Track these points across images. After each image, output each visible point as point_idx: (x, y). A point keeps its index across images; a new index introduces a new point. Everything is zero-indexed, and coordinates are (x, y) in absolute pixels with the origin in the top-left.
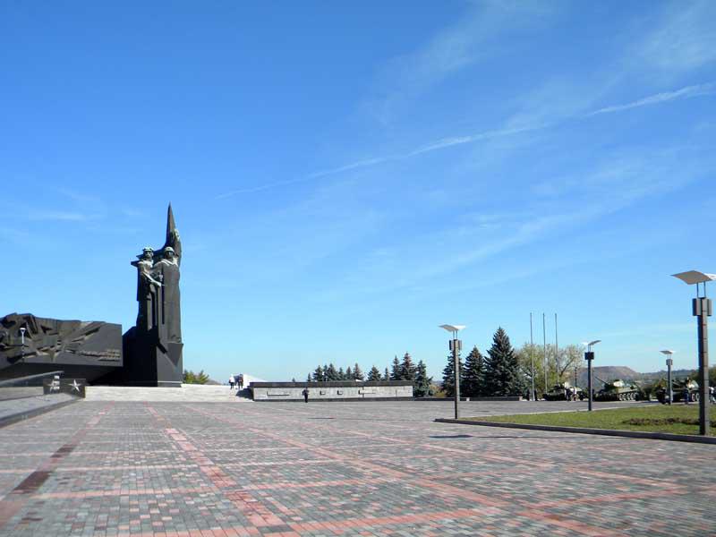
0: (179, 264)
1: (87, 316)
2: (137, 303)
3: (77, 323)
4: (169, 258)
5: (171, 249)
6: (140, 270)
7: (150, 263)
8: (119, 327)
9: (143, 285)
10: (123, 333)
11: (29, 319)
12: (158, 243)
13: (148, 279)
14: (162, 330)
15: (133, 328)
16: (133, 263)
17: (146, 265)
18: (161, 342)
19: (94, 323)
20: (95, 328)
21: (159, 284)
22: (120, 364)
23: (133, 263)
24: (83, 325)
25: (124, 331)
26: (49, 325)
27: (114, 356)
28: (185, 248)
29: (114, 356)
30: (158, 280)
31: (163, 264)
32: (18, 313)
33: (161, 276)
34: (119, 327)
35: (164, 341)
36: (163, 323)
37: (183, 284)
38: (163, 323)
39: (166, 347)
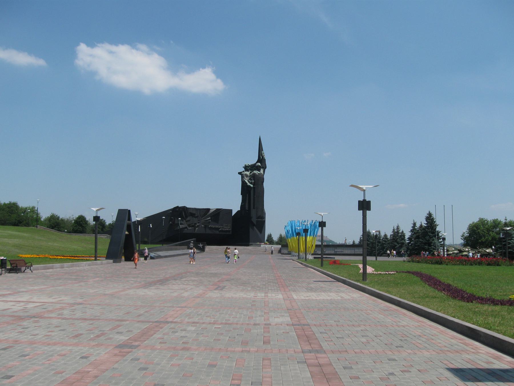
0: (264, 173)
1: (213, 206)
3: (208, 210)
4: (259, 170)
5: (259, 164)
6: (242, 177)
7: (248, 173)
8: (231, 211)
10: (233, 214)
11: (184, 209)
12: (253, 160)
13: (246, 183)
14: (253, 213)
17: (246, 174)
19: (217, 209)
20: (219, 212)
21: (252, 186)
22: (231, 233)
24: (211, 211)
25: (233, 214)
26: (194, 212)
27: (227, 227)
28: (268, 163)
29: (227, 227)
30: (251, 183)
31: (254, 174)
32: (180, 206)
33: (253, 181)
34: (231, 211)
35: (254, 220)
36: (254, 208)
37: (266, 185)
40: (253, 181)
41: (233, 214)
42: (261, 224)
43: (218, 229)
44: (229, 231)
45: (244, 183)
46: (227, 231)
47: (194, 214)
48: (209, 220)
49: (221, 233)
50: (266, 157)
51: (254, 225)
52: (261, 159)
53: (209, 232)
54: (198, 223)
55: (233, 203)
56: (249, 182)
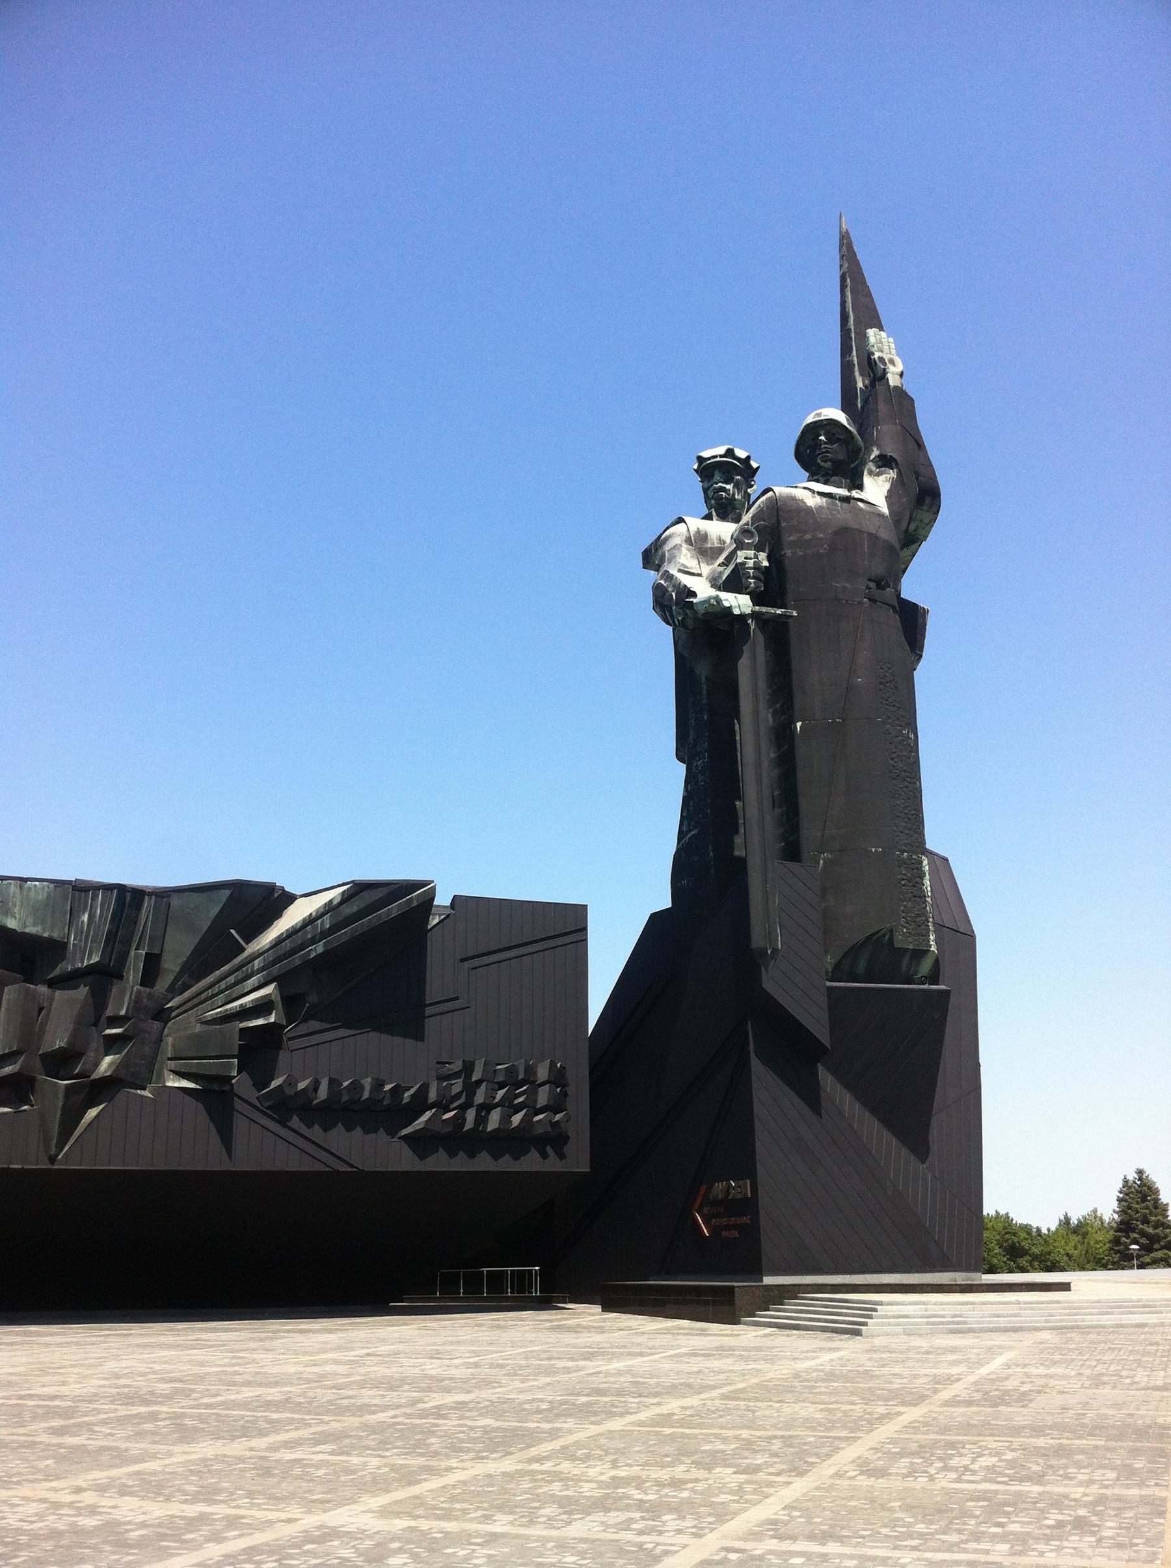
2: (682, 768)
8: (566, 927)
15: (656, 920)
18: (774, 982)
19: (359, 888)
21: (740, 603)
22: (578, 1159)
30: (734, 583)
33: (753, 558)
35: (800, 985)
38: (792, 852)
39: (815, 1020)
40: (753, 558)
43: (387, 1113)
44: (556, 1140)
46: (510, 1142)
47: (57, 948)
48: (262, 1008)
49: (439, 1162)
51: (796, 1054)
53: (264, 1147)
54: (111, 1044)
56: (714, 583)
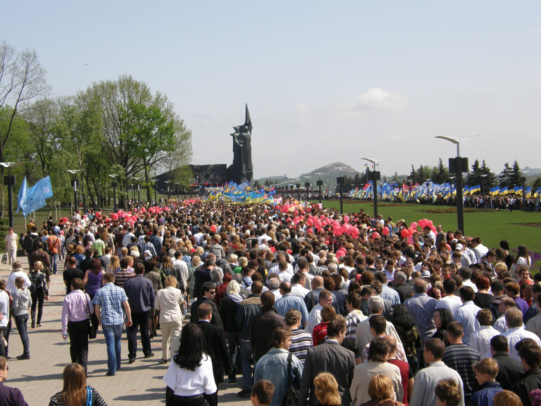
4: (246, 132)
5: (247, 127)
7: (238, 134)
9: (235, 145)
12: (243, 123)
14: (244, 166)
16: (231, 135)
19: (216, 165)
21: (242, 145)
23: (231, 135)
24: (211, 167)
25: (227, 167)
28: (253, 125)
34: (225, 165)
35: (244, 172)
37: (253, 144)
41: (227, 167)
42: (249, 176)
45: (235, 143)
50: (252, 121)
51: (244, 176)
52: (248, 123)
55: (228, 160)
